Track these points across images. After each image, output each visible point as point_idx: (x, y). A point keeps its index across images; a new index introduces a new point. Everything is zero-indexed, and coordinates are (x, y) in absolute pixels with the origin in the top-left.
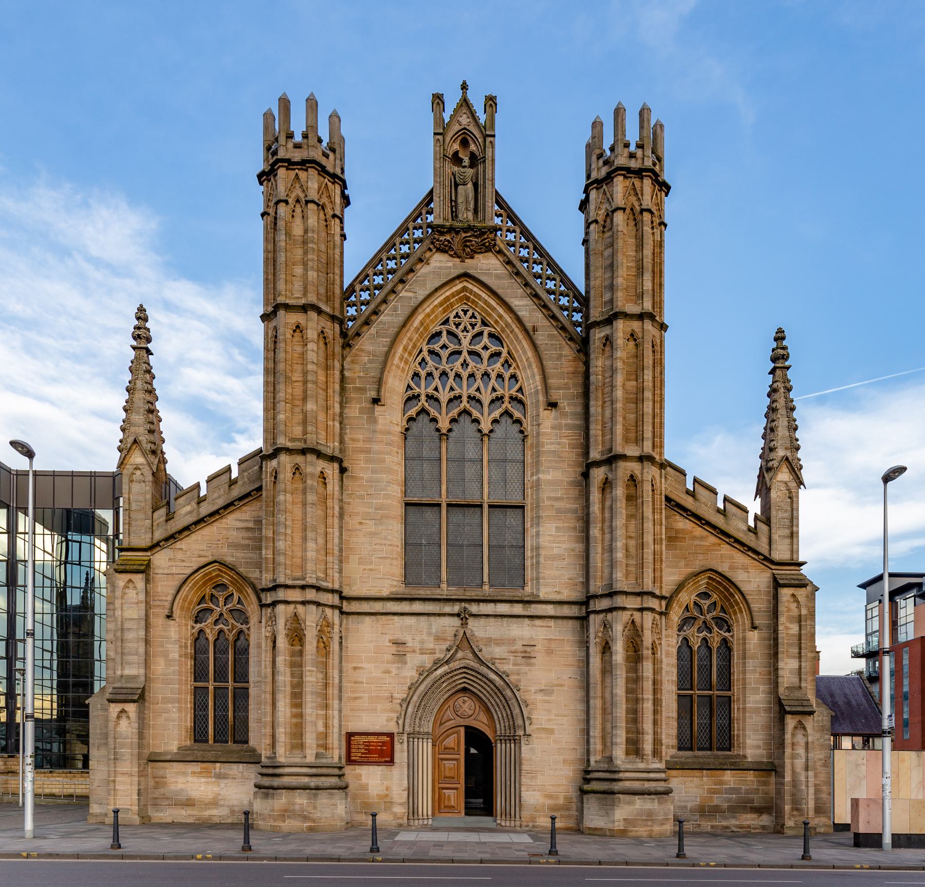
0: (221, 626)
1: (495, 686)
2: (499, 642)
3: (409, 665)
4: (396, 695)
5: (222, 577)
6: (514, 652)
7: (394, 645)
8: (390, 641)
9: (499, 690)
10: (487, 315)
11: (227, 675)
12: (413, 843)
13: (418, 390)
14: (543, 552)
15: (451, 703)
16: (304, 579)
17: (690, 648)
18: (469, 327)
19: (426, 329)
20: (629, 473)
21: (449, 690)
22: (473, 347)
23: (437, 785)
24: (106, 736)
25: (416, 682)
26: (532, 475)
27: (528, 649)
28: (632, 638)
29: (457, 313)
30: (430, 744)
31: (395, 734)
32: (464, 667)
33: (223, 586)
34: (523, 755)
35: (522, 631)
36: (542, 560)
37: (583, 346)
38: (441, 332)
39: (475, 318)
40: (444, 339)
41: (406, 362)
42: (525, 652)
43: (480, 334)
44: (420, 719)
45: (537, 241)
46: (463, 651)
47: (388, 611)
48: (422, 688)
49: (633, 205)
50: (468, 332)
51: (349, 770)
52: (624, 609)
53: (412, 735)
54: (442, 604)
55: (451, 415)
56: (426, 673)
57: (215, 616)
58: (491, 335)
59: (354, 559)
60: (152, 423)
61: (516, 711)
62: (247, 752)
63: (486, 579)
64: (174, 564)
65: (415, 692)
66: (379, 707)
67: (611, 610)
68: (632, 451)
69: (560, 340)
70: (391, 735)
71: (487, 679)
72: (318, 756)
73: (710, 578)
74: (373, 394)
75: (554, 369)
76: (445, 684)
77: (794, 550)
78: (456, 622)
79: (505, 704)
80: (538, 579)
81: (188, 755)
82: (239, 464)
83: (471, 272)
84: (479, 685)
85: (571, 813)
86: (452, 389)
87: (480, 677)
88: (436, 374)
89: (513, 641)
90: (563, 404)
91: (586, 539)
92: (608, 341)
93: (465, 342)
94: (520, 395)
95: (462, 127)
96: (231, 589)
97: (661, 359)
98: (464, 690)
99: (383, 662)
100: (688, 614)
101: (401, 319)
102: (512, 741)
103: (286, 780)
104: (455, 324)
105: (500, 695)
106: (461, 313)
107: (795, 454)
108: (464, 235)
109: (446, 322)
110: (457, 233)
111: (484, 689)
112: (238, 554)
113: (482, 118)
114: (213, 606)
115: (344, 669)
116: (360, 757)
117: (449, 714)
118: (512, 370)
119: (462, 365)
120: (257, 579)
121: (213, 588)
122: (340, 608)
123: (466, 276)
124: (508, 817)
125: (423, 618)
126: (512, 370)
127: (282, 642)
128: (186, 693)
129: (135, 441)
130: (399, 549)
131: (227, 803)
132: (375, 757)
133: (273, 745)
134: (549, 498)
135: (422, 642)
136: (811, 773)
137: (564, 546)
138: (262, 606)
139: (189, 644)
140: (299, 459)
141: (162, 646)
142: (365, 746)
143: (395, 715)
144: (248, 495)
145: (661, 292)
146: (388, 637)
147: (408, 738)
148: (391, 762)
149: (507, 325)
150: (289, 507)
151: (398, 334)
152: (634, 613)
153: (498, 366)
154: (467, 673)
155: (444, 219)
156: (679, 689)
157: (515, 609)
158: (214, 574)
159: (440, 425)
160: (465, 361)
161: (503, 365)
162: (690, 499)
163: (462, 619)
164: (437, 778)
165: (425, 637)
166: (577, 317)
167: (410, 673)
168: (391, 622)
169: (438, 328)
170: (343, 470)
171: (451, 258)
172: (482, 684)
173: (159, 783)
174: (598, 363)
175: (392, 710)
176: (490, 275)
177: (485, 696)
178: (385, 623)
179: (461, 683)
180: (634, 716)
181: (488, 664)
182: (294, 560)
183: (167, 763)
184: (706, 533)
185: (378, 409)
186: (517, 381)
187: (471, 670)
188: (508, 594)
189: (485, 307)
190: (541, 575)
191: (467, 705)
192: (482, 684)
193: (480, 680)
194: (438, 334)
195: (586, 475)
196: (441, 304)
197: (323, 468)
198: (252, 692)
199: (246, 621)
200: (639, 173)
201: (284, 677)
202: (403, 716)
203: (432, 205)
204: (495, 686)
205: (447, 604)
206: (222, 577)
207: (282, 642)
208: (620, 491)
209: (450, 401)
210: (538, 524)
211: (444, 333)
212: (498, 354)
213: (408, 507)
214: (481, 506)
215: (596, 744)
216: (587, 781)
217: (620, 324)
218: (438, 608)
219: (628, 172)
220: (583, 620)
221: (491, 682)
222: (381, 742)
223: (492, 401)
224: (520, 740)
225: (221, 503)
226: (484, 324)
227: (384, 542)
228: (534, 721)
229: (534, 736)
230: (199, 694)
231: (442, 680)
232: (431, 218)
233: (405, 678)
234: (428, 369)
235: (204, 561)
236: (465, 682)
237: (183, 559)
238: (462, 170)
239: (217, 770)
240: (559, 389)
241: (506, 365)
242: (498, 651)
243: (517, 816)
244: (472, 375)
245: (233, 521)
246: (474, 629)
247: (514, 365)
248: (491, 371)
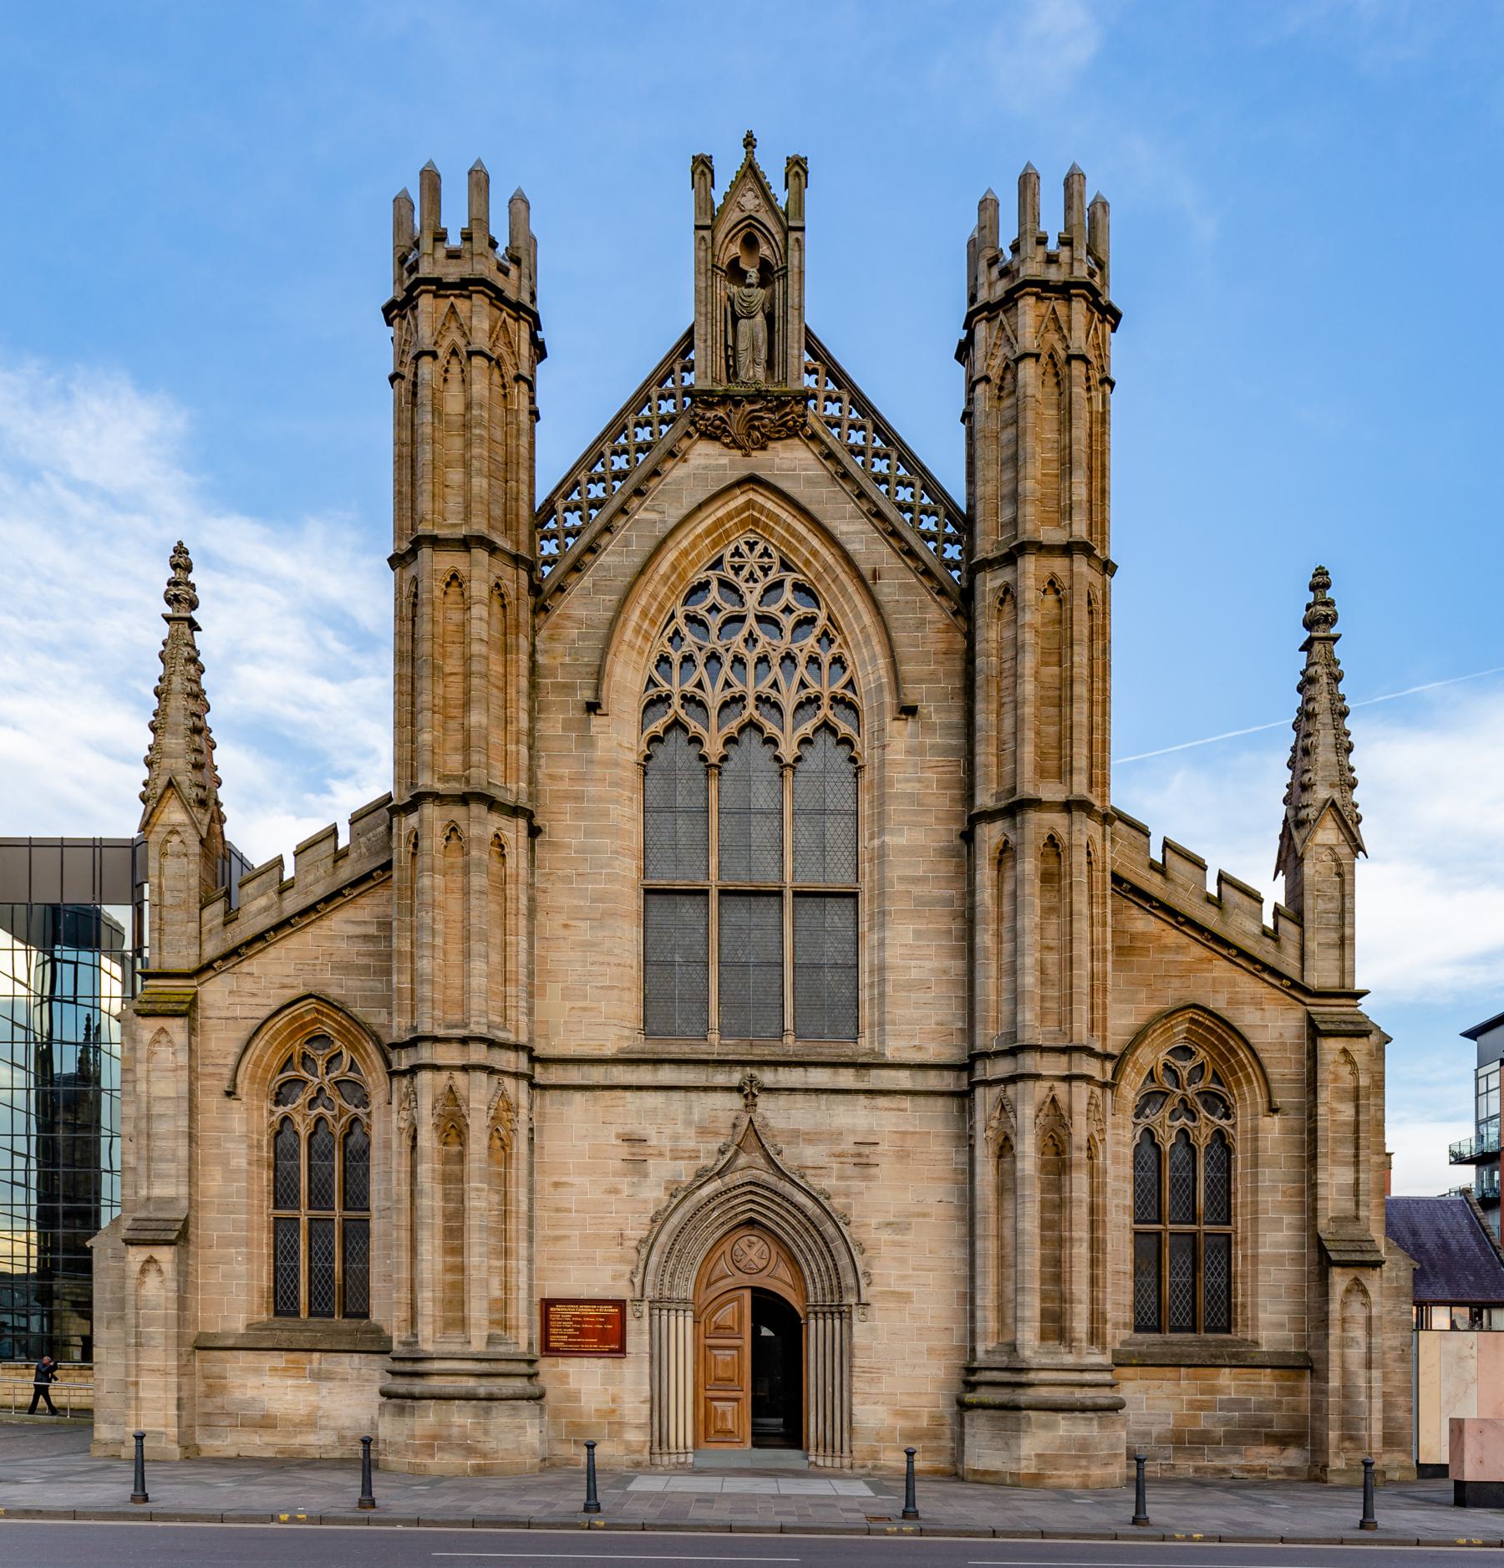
0: (321, 1110)
1: (806, 1216)
2: (812, 1138)
3: (652, 1178)
4: (628, 1233)
5: (322, 1023)
7: (626, 1144)
8: (618, 1136)
9: (812, 1223)
10: (791, 551)
11: (331, 1197)
12: (660, 1496)
13: (667, 687)
14: (890, 976)
15: (726, 1247)
16: (466, 1026)
17: (1157, 1147)
18: (759, 573)
19: (681, 578)
20: (1046, 832)
22: (765, 609)
23: (702, 1394)
24: (121, 1304)
25: (665, 1210)
26: (871, 838)
27: (866, 1150)
28: (1053, 1130)
29: (737, 548)
30: (690, 1321)
31: (628, 1302)
32: (751, 1183)
33: (324, 1039)
34: (855, 1340)
35: (854, 1117)
36: (889, 989)
37: (963, 604)
38: (708, 583)
39: (770, 556)
40: (714, 595)
41: (646, 638)
42: (859, 1155)
43: (779, 584)
44: (672, 1275)
45: (880, 417)
46: (749, 1154)
47: (615, 1082)
48: (675, 1220)
49: (1053, 348)
50: (756, 581)
51: (545, 1366)
52: (1037, 1077)
53: (658, 1304)
54: (710, 1070)
55: (725, 730)
56: (683, 1194)
57: (310, 1093)
58: (798, 587)
59: (554, 990)
60: (199, 751)
61: (844, 1261)
62: (366, 1332)
63: (789, 1025)
64: (238, 1000)
65: (662, 1226)
66: (599, 1253)
67: (1013, 1079)
68: (1052, 792)
69: (922, 594)
70: (620, 1304)
71: (792, 1203)
72: (491, 1340)
73: (1192, 1021)
74: (588, 695)
75: (911, 646)
76: (716, 1214)
77: (1345, 969)
78: (737, 1101)
79: (824, 1249)
80: (882, 1024)
81: (263, 1338)
82: (352, 823)
83: (761, 473)
84: (778, 1214)
85: (943, 1443)
86: (728, 684)
87: (778, 1200)
88: (700, 658)
89: (836, 1136)
90: (927, 708)
91: (969, 952)
92: (1008, 594)
93: (752, 600)
94: (850, 694)
95: (746, 214)
96: (338, 1043)
97: (1104, 626)
98: (751, 1223)
99: (606, 1174)
100: (1153, 1087)
101: (638, 560)
102: (836, 1315)
103: (435, 1384)
104: (733, 567)
105: (814, 1233)
106: (744, 549)
107: (1348, 795)
108: (749, 408)
109: (717, 564)
110: (737, 404)
111: (787, 1221)
112: (350, 983)
113: (782, 197)
114: (306, 1075)
115: (537, 1187)
116: (566, 1343)
117: (724, 1266)
118: (834, 650)
119: (746, 641)
120: (383, 1026)
121: (307, 1043)
122: (530, 1078)
123: (752, 481)
124: (829, 1450)
125: (677, 1096)
126: (834, 650)
127: (428, 1139)
128: (260, 1229)
129: (170, 784)
130: (634, 972)
131: (332, 1424)
132: (593, 1343)
133: (413, 1321)
134: (902, 879)
135: (675, 1138)
136: (1376, 1374)
137: (928, 964)
138: (393, 1074)
139: (265, 1143)
140: (457, 812)
141: (218, 1146)
142: (575, 1322)
143: (627, 1269)
144: (367, 877)
145: (1103, 504)
147: (651, 1309)
148: (621, 1351)
149: (827, 568)
150: (440, 898)
151: (632, 586)
152: (1056, 1084)
153: (810, 642)
154: (756, 1194)
155: (714, 379)
156: (1136, 1222)
158: (308, 1018)
159: (706, 749)
160: (751, 634)
161: (819, 641)
162: (1157, 878)
163: (746, 1096)
164: (701, 1380)
165: (680, 1128)
166: (953, 552)
167: (654, 1194)
168: (620, 1102)
169: (703, 576)
170: (534, 832)
171: (726, 450)
172: (783, 1212)
173: (215, 1386)
174: (990, 634)
175: (622, 1260)
176: (796, 478)
177: (788, 1234)
178: (609, 1103)
179: (744, 1212)
180: (1056, 1271)
181: (793, 1176)
182: (449, 992)
183: (228, 1353)
184: (1186, 940)
185: (596, 721)
186: (844, 669)
187: (763, 1187)
188: (828, 1051)
189: (787, 535)
190: (888, 1017)
191: (755, 1250)
192: (783, 1212)
193: (778, 1205)
194: (704, 586)
195: (968, 837)
196: (708, 532)
197: (499, 829)
198: (376, 1226)
199: (364, 1102)
200: (1064, 291)
201: (432, 1201)
202: (641, 1270)
203: (692, 356)
204: (806, 1216)
205: (720, 1069)
206: (322, 1023)
207: (428, 1139)
208: (1030, 866)
209: (725, 705)
210: (882, 926)
211: (714, 584)
212: (810, 621)
213: (649, 897)
214: (779, 894)
215: (988, 1321)
216: (971, 1386)
217: (1030, 565)
218: (704, 1077)
219: (1043, 288)
220: (964, 1098)
221: (799, 1209)
222: (602, 1316)
223: (800, 706)
224: (850, 1312)
225: (320, 891)
226: (786, 566)
227: (607, 959)
228: (875, 1279)
229: (876, 1305)
230: (283, 1231)
231: (711, 1206)
232: (690, 379)
233: (645, 1201)
234: (685, 649)
235: (290, 994)
236: (751, 1210)
237: (255, 991)
238: (746, 291)
239: (315, 1365)
240: (920, 681)
241: (825, 640)
242: (810, 1154)
243: (846, 1449)
244: (763, 660)
245: (342, 924)
246: (768, 1114)
247: (839, 640)
248: (797, 651)
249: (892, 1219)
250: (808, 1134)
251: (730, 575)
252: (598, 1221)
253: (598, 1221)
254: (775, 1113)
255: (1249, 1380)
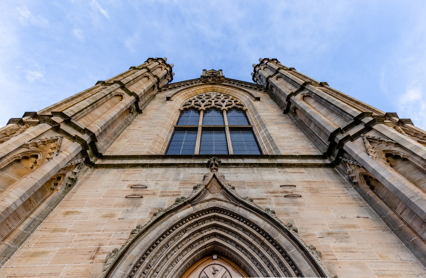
2: (254, 185)
6: (273, 193)
45: (238, 81)
146: (128, 183)
154: (219, 218)
196: (203, 89)
236: (215, 235)
249: (330, 230)
250: (250, 183)
252: (86, 238)
253: (86, 238)
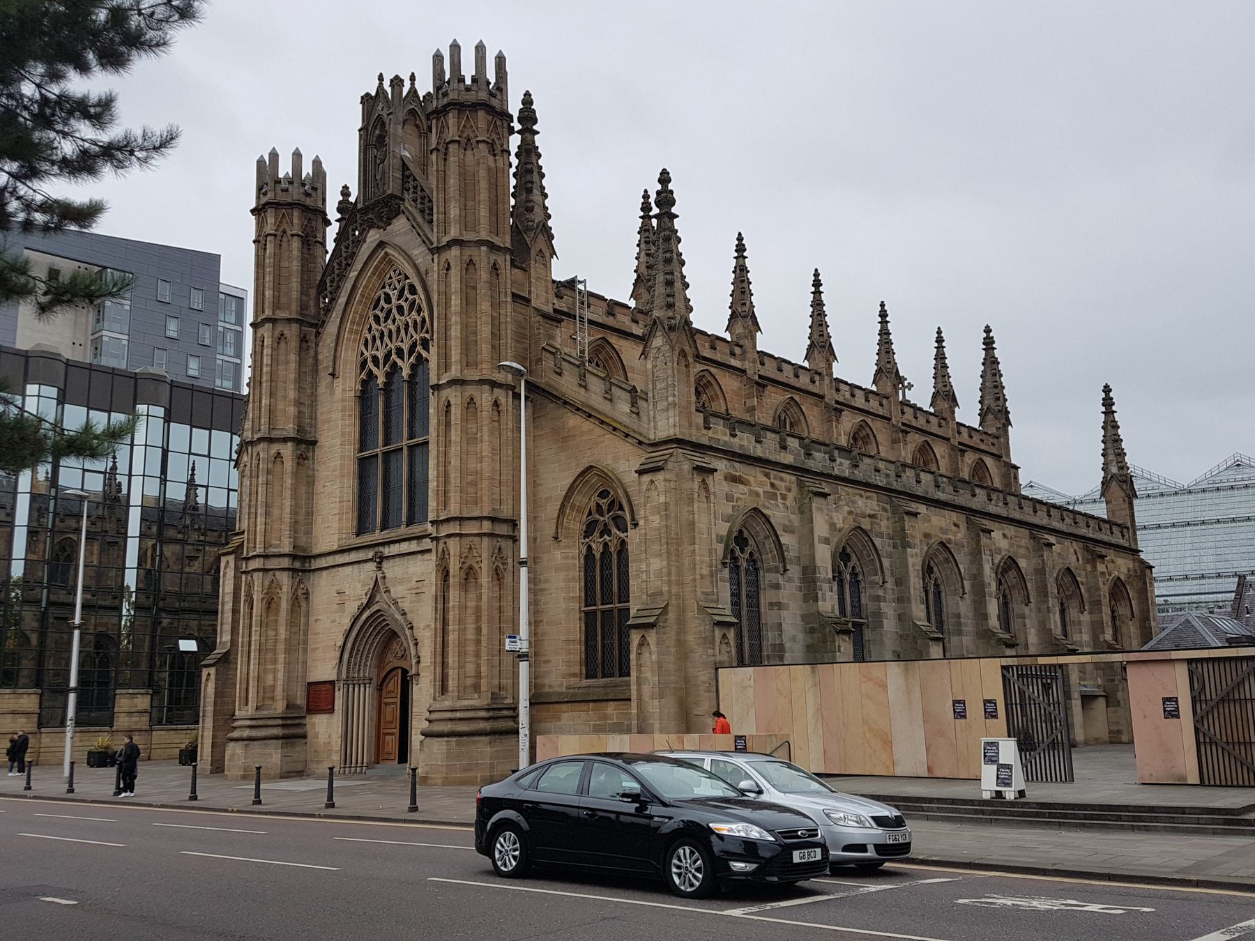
2: (401, 581)
18: (397, 284)
21: (377, 634)
41: (356, 333)
42: (418, 588)
53: (350, 682)
70: (332, 683)
74: (330, 371)
117: (390, 657)
125: (356, 566)
157: (412, 546)
185: (336, 381)
196: (373, 274)
211: (383, 296)
251: (387, 290)
254: (392, 570)
255: (623, 709)
